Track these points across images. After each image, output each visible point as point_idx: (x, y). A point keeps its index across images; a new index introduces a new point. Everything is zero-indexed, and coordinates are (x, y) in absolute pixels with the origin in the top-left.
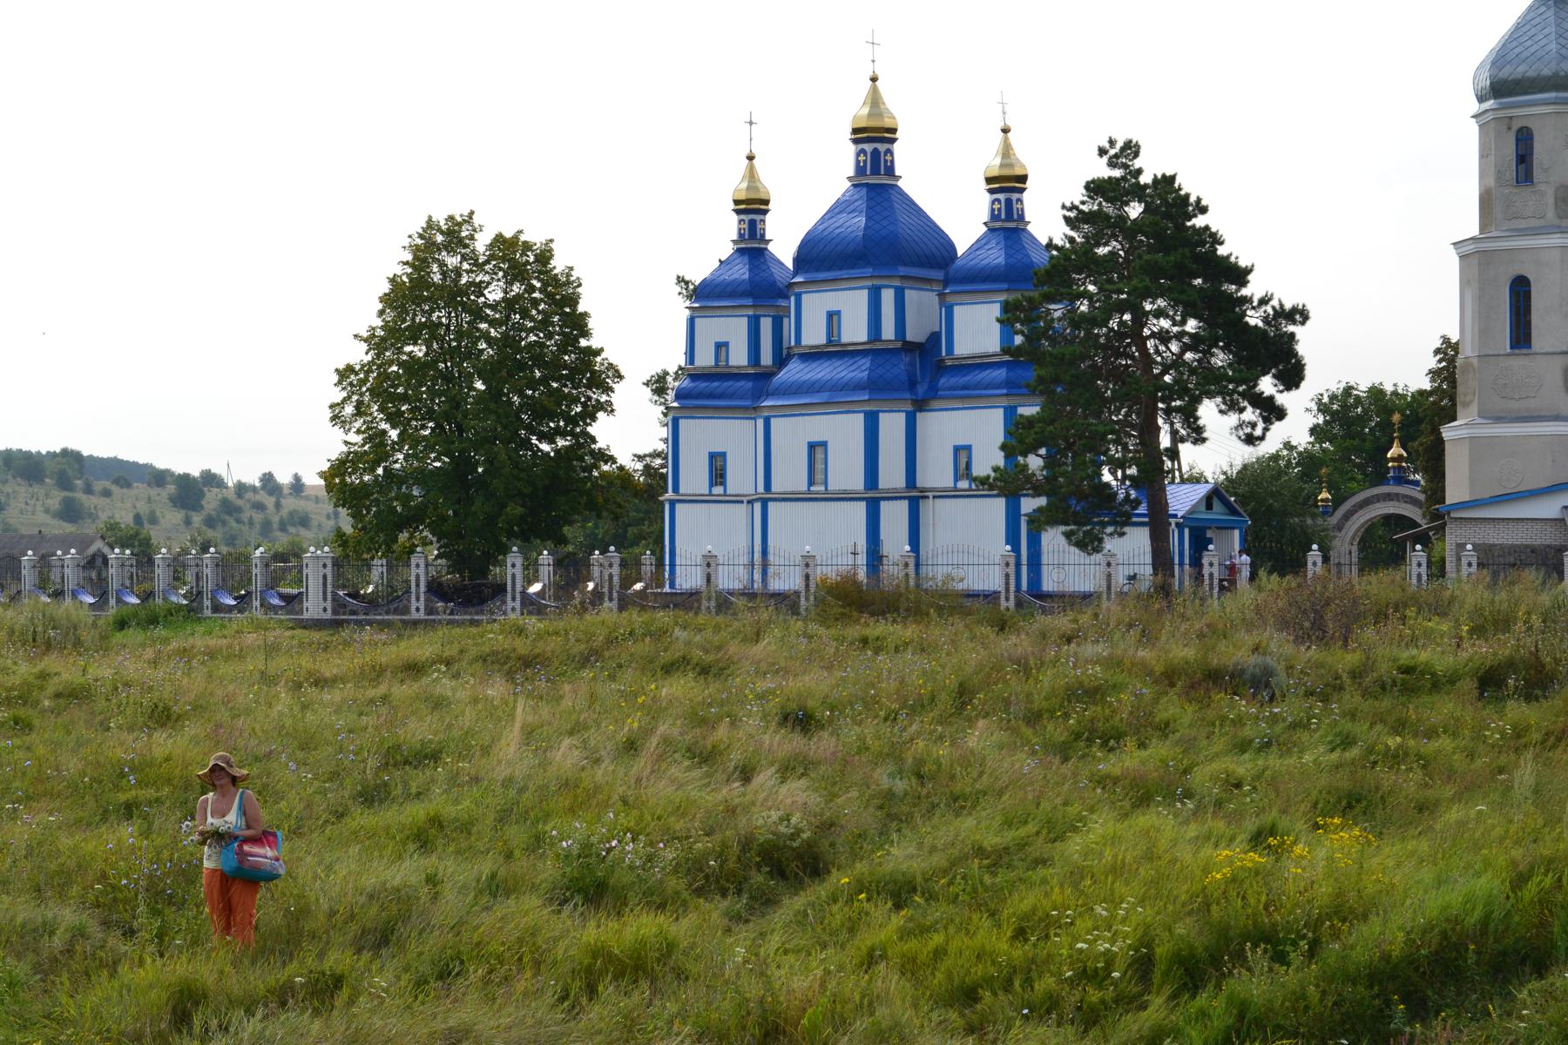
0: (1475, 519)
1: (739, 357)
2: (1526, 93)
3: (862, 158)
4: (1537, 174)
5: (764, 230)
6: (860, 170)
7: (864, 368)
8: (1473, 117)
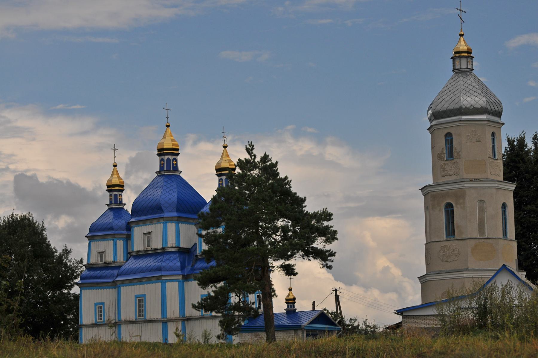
0: (415, 316)
1: (109, 258)
2: (448, 117)
3: (162, 163)
5: (121, 199)
6: (161, 168)
7: (160, 261)
8: (427, 130)
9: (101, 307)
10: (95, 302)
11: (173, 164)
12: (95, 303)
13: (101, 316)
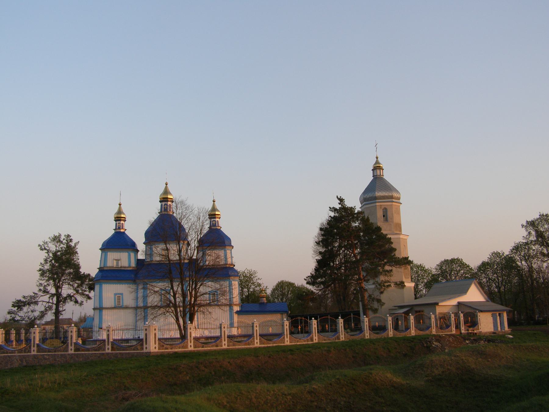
4: (389, 219)
9: (119, 297)
10: (115, 293)
11: (164, 207)
12: (114, 294)
13: (119, 302)
